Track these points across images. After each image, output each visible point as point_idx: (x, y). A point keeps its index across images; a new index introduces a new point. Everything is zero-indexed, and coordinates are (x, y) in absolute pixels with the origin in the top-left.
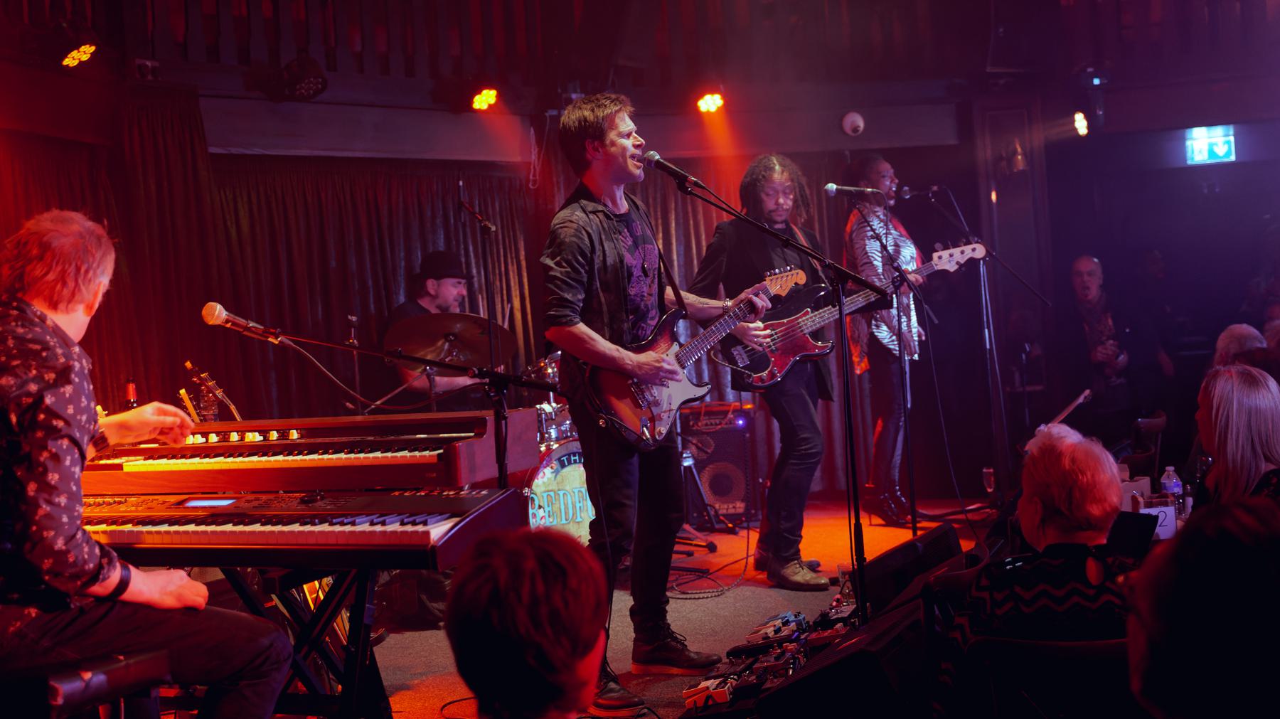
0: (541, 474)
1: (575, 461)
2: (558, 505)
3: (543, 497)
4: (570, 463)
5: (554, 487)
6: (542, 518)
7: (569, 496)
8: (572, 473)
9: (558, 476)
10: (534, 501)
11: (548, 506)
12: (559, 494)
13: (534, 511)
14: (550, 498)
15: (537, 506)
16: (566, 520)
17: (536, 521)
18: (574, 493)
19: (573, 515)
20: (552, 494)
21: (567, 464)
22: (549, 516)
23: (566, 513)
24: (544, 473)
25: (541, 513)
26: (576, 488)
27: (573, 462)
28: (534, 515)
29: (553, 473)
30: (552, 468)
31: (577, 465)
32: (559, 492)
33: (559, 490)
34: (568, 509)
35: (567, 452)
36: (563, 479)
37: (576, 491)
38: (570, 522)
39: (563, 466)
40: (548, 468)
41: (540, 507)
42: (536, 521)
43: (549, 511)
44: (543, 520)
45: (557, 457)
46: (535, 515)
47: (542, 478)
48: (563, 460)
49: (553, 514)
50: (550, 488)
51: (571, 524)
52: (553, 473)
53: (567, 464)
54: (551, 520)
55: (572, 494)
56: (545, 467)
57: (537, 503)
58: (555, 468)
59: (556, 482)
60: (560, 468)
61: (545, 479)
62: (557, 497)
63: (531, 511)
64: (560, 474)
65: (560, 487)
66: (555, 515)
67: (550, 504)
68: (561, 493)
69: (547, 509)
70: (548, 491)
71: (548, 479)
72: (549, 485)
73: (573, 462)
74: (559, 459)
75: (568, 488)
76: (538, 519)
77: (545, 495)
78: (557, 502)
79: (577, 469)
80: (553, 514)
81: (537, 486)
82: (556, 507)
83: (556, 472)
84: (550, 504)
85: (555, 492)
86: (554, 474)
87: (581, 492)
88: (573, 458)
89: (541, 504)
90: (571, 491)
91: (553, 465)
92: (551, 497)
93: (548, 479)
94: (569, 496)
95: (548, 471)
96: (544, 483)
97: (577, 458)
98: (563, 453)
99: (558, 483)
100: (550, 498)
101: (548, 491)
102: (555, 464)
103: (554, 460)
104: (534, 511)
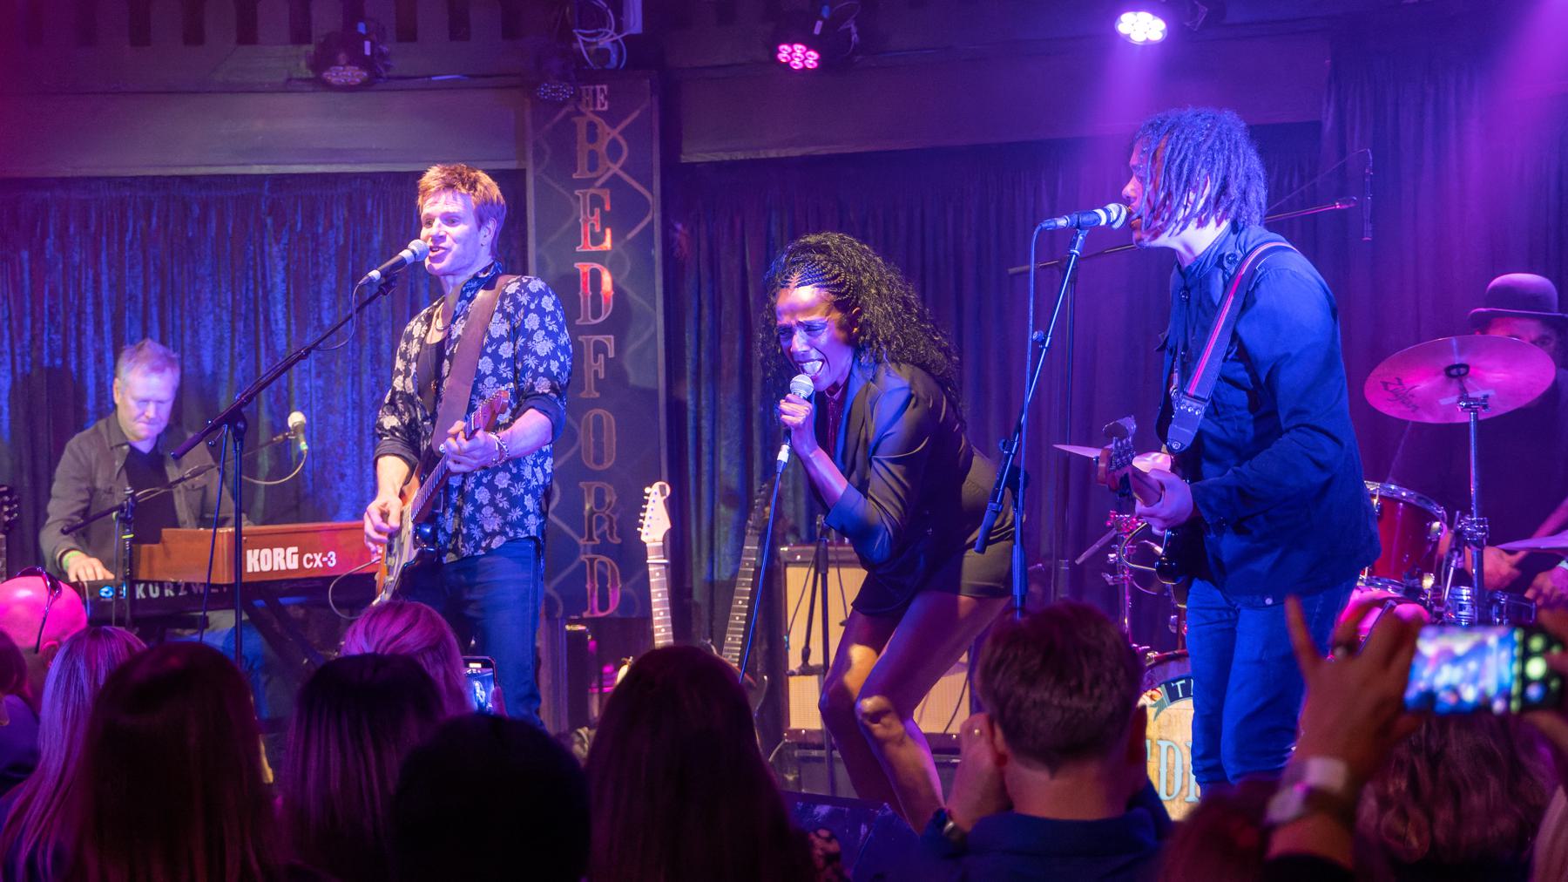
7: (1177, 750)
9: (1161, 714)
12: (1159, 746)
16: (1168, 795)
19: (1182, 788)
21: (1181, 695)
23: (1168, 782)
32: (1160, 743)
33: (1161, 739)
34: (1173, 775)
35: (1185, 674)
38: (1174, 799)
39: (1173, 697)
45: (1164, 680)
48: (1177, 686)
51: (1177, 799)
53: (1181, 695)
58: (1158, 699)
60: (1165, 697)
62: (1155, 750)
64: (1165, 710)
65: (1164, 735)
68: (1164, 745)
90: (1182, 744)
91: (1154, 693)
98: (1177, 676)
99: (1159, 727)
102: (1160, 693)
103: (1157, 684)
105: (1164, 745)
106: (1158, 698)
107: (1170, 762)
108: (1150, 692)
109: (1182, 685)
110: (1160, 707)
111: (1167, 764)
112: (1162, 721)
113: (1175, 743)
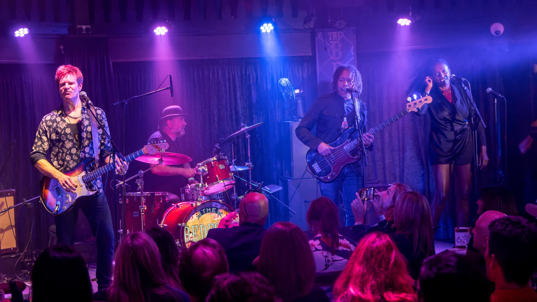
0: (191, 217)
1: (209, 211)
2: (200, 232)
3: (192, 228)
4: (206, 212)
5: (198, 223)
6: (191, 238)
7: (205, 226)
8: (207, 217)
10: (187, 230)
11: (195, 232)
13: (187, 234)
14: (195, 228)
15: (189, 232)
17: (188, 239)
18: (208, 226)
20: (197, 226)
22: (195, 237)
24: (193, 217)
25: (191, 235)
26: (209, 224)
27: (207, 212)
28: (187, 236)
29: (197, 217)
30: (197, 214)
31: (210, 213)
32: (200, 226)
33: (200, 225)
36: (202, 220)
37: (209, 225)
39: (202, 213)
40: (194, 214)
41: (190, 232)
42: (188, 239)
43: (195, 234)
44: (192, 238)
45: (199, 210)
46: (188, 236)
47: (192, 219)
49: (197, 235)
50: (196, 224)
52: (197, 217)
54: (196, 238)
55: (207, 226)
56: (193, 214)
57: (189, 231)
59: (199, 221)
61: (193, 220)
62: (199, 228)
63: (185, 235)
65: (201, 223)
66: (198, 236)
67: (196, 231)
68: (201, 226)
69: (194, 233)
70: (195, 225)
71: (195, 219)
72: (195, 223)
73: (207, 212)
74: (200, 210)
75: (205, 224)
76: (189, 238)
77: (193, 227)
78: (199, 230)
79: (210, 215)
80: (197, 235)
81: (189, 223)
82: (198, 233)
83: (199, 217)
84: (196, 231)
85: (198, 226)
86: (198, 217)
87: (212, 225)
88: (207, 210)
89: (191, 231)
91: (197, 213)
92: (196, 227)
93: (195, 219)
94: (205, 226)
95: (195, 216)
96: (192, 222)
97: (210, 210)
99: (200, 222)
100: (195, 228)
101: (195, 225)
102: (199, 213)
103: (197, 211)
104: (187, 234)
105: (201, 226)
106: (198, 214)
107: (204, 230)
108: (196, 213)
109: (204, 210)
110: (199, 217)
111: (203, 231)
112: (200, 220)
113: (204, 225)
